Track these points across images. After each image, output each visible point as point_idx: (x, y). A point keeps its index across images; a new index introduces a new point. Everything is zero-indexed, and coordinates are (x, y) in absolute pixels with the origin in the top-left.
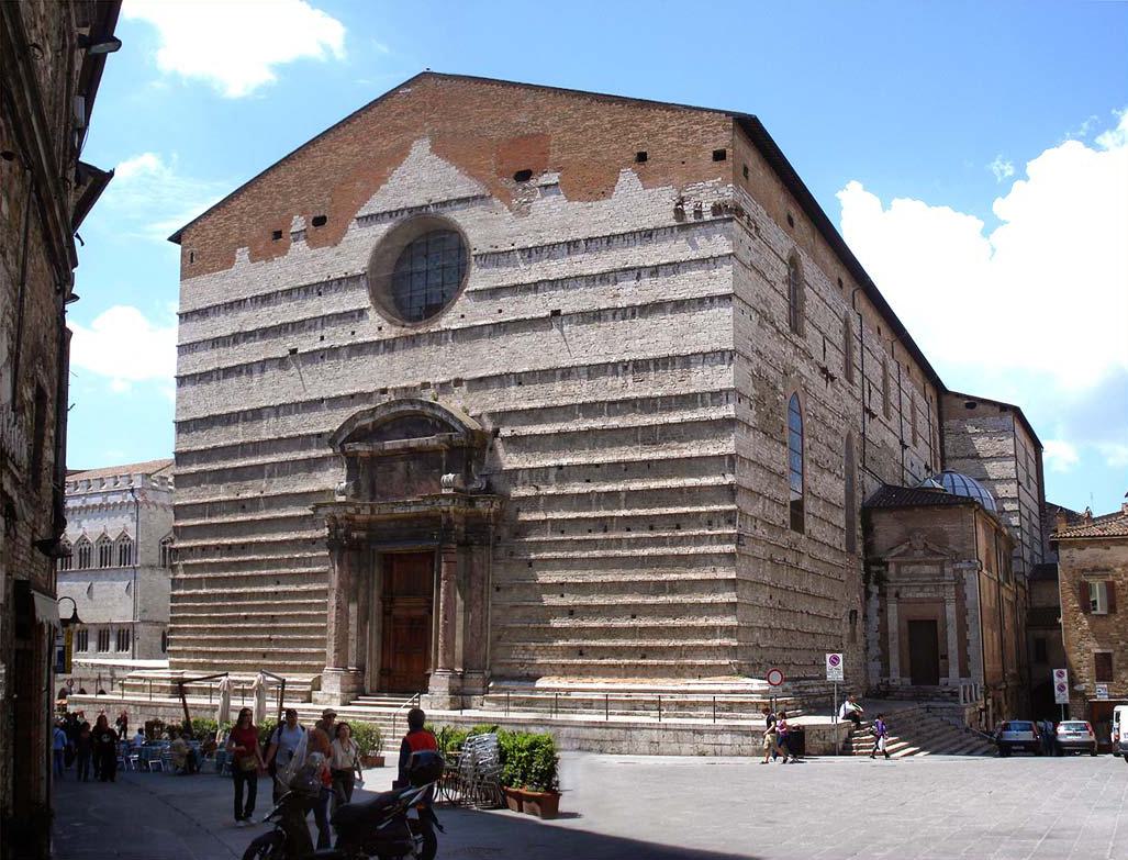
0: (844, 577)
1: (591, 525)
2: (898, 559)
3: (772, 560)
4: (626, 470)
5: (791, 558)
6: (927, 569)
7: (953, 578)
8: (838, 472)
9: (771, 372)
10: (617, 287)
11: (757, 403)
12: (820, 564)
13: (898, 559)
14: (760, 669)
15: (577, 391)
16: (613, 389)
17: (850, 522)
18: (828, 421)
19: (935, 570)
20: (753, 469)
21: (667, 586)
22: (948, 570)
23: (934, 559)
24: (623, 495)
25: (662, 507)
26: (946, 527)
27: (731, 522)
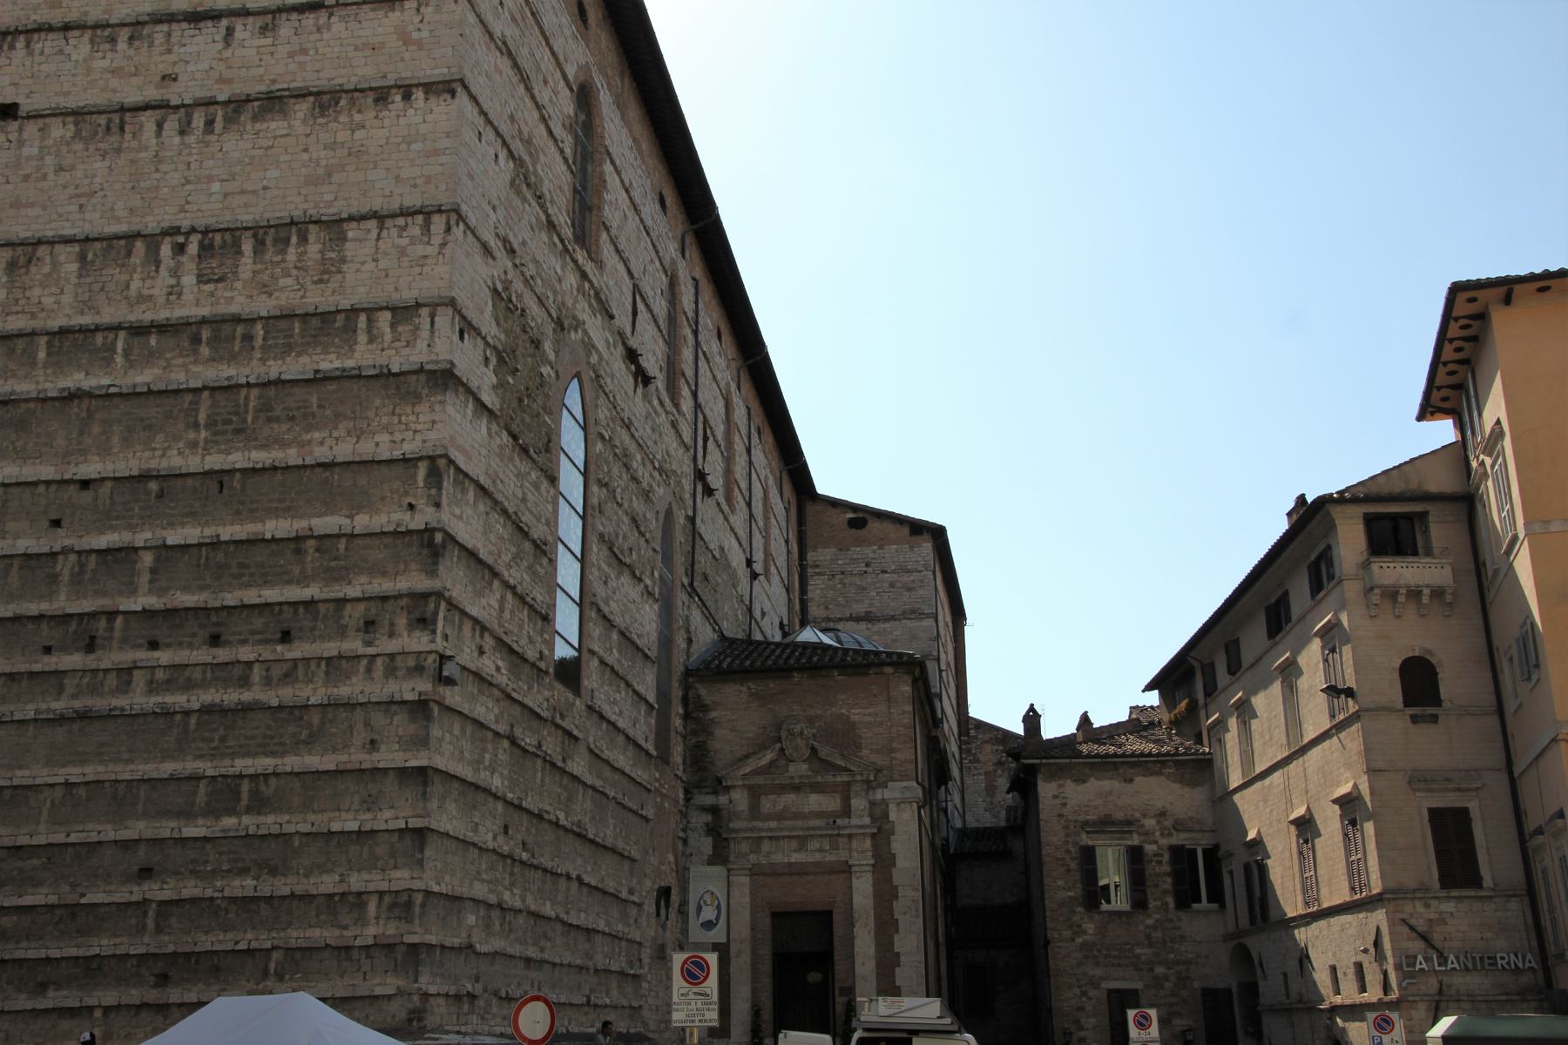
0: (649, 812)
1: (46, 633)
2: (759, 780)
3: (513, 742)
4: (161, 495)
5: (552, 746)
6: (815, 801)
7: (867, 821)
8: (648, 582)
9: (533, 308)
10: (173, 58)
11: (501, 360)
12: (608, 773)
13: (759, 780)
14: (471, 1012)
15: (48, 301)
16: (143, 299)
17: (663, 694)
18: (635, 465)
19: (831, 803)
20: (482, 508)
21: (245, 787)
22: (858, 803)
23: (830, 778)
24: (147, 559)
25: (248, 586)
26: (856, 715)
27: (424, 622)
